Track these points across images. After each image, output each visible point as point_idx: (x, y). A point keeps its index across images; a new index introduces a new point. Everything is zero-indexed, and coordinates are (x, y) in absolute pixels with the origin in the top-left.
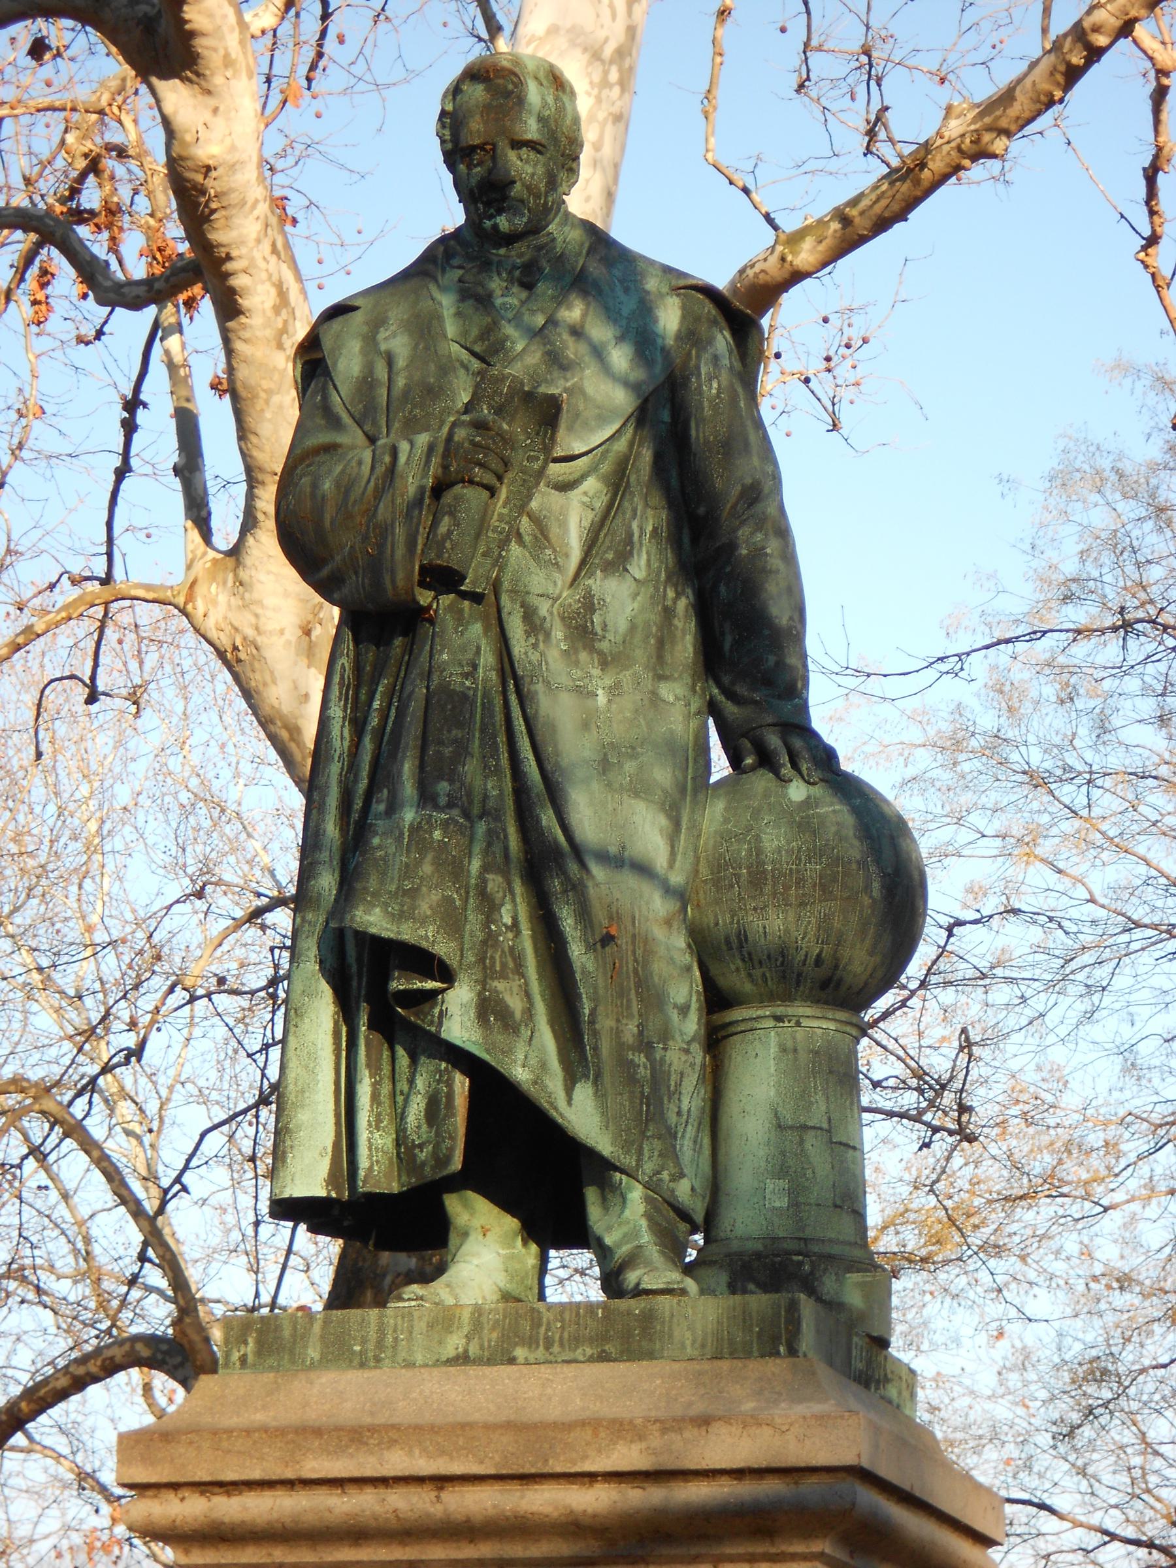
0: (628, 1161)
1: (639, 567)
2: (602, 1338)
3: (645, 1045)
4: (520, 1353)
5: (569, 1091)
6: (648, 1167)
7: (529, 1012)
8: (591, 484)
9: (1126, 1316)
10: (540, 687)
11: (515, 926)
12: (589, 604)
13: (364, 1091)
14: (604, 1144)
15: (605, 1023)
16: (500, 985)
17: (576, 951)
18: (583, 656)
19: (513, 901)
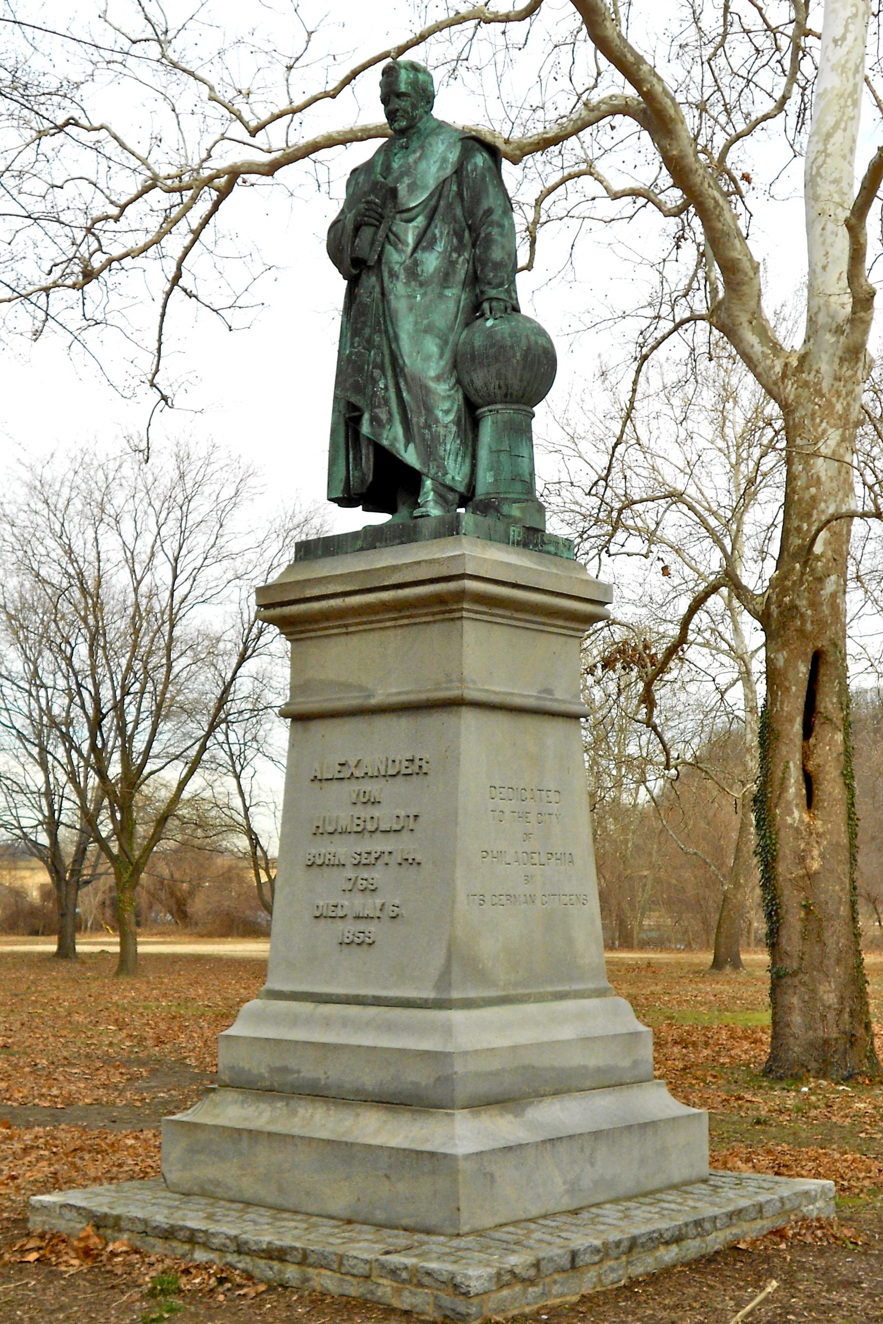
0: (425, 470)
1: (439, 247)
2: (402, 536)
3: (429, 427)
4: (378, 544)
5: (406, 447)
6: (433, 471)
7: (390, 420)
8: (420, 219)
9: (60, 506)
10: (392, 297)
11: (386, 388)
12: (416, 263)
13: (351, 456)
14: (417, 465)
15: (415, 420)
16: (377, 410)
17: (405, 394)
18: (413, 283)
19: (386, 378)
